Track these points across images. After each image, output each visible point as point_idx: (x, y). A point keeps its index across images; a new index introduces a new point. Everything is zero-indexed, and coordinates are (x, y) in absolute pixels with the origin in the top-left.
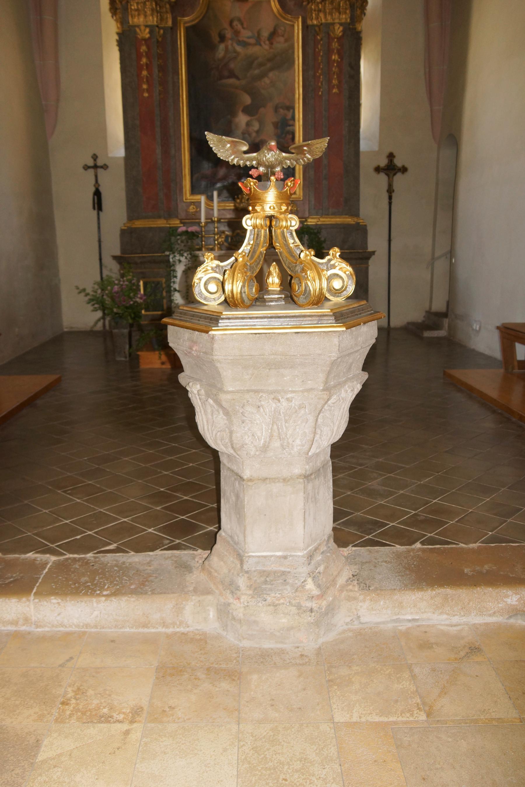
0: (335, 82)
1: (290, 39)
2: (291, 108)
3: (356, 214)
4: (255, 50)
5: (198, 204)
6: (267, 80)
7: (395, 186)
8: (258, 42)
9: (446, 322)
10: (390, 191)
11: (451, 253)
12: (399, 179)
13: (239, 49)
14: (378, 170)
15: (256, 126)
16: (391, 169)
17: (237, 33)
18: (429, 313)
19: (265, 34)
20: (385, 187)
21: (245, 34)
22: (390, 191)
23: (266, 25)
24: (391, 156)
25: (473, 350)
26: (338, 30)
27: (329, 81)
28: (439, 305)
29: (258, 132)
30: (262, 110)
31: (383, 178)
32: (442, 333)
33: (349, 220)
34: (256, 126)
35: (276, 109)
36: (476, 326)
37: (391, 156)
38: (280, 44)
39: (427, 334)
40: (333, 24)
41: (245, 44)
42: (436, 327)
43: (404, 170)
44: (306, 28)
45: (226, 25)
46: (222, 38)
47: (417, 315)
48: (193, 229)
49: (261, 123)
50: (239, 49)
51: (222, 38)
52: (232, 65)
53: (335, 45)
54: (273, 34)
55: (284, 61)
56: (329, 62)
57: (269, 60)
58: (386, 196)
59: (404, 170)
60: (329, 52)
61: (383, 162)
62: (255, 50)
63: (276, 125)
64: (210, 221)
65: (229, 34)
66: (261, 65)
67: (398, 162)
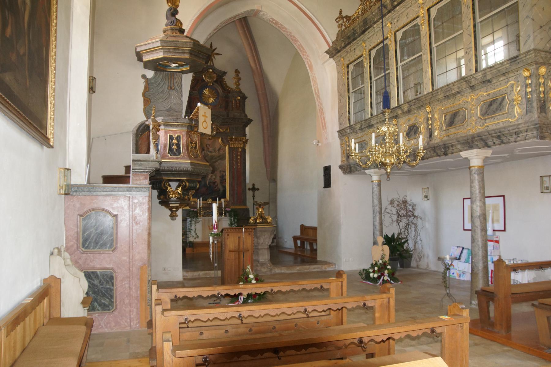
1: (225, 150)
2: (225, 172)
3: (245, 205)
4: (214, 154)
5: (196, 202)
6: (217, 163)
7: (255, 195)
8: (215, 151)
12: (256, 192)
13: (209, 153)
14: (249, 189)
15: (214, 177)
16: (254, 189)
17: (208, 148)
19: (217, 149)
21: (211, 149)
24: (254, 185)
26: (240, 150)
27: (237, 164)
30: (216, 172)
31: (251, 192)
33: (244, 207)
34: (214, 177)
35: (220, 172)
36: (286, 240)
37: (254, 185)
38: (221, 152)
40: (238, 148)
43: (258, 189)
44: (229, 148)
48: (195, 210)
49: (216, 176)
50: (209, 153)
53: (239, 154)
54: (219, 150)
55: (223, 157)
57: (219, 157)
58: (252, 198)
59: (258, 189)
60: (237, 156)
61: (251, 187)
62: (214, 154)
63: (220, 177)
64: (200, 207)
65: (206, 149)
66: (215, 158)
67: (256, 187)
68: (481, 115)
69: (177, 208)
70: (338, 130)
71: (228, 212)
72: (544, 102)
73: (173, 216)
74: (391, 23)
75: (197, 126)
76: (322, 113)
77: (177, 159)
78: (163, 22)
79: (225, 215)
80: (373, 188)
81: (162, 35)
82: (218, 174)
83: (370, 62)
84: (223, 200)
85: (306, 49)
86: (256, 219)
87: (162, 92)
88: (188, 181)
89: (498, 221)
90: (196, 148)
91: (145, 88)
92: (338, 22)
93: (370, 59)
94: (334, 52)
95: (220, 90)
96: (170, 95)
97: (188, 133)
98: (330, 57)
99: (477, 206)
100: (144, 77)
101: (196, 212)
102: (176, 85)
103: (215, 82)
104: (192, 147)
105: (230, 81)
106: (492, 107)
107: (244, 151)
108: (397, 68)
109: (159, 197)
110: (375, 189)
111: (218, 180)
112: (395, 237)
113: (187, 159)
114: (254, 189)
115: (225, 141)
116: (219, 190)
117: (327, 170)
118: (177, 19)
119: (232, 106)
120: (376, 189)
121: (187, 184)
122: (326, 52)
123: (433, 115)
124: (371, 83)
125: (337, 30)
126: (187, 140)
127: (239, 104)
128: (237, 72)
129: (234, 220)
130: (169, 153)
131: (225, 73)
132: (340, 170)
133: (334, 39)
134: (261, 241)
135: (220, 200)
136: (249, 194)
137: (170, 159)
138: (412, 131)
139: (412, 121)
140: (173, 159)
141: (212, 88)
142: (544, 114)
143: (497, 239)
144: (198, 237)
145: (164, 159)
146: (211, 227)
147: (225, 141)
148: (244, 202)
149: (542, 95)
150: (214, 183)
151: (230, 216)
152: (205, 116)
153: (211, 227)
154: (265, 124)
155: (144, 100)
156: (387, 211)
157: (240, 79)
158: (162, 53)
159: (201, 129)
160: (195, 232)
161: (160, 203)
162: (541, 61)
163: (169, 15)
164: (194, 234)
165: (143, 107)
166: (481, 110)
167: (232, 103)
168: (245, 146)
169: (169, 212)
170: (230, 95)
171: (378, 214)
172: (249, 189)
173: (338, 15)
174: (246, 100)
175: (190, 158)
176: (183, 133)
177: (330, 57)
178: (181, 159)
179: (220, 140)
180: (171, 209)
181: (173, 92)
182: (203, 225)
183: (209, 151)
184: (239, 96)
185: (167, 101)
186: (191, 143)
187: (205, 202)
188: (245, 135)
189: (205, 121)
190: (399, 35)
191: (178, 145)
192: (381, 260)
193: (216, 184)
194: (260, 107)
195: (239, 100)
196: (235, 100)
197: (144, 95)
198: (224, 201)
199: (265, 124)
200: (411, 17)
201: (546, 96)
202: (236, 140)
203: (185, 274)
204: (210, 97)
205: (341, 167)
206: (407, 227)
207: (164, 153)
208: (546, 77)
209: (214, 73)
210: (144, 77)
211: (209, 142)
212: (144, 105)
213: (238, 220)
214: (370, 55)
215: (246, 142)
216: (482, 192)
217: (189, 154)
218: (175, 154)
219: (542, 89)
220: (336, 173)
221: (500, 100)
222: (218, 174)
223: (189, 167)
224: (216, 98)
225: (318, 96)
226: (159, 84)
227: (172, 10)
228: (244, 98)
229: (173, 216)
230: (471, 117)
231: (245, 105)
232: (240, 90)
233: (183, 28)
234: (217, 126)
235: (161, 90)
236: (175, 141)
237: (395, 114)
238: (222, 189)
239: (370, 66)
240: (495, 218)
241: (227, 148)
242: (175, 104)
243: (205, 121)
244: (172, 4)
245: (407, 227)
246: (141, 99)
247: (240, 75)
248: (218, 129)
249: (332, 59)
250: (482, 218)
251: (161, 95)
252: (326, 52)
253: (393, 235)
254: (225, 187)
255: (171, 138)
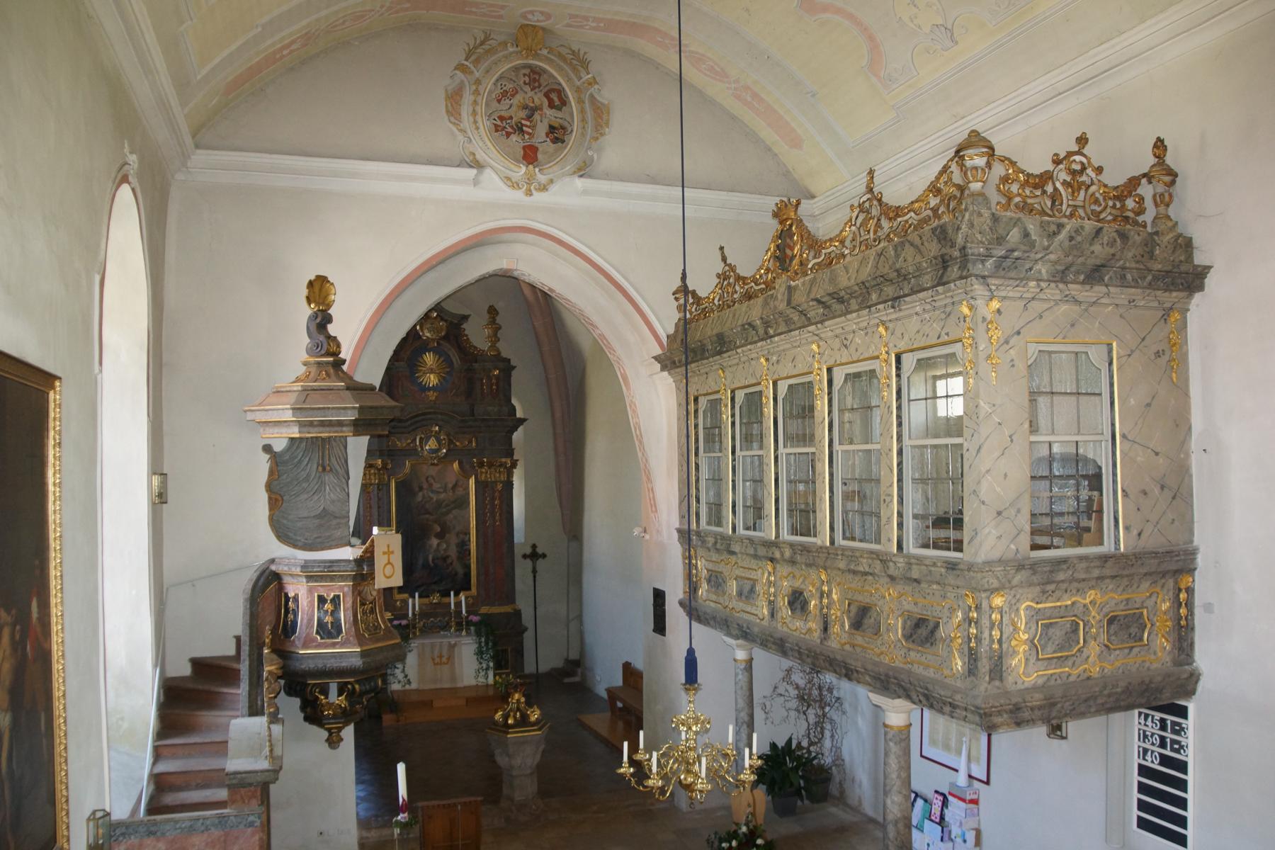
0: (497, 517)
2: (468, 533)
5: (405, 602)
6: (451, 516)
7: (538, 569)
8: (445, 491)
9: (579, 671)
10: (534, 571)
11: (580, 617)
12: (540, 562)
14: (525, 556)
16: (534, 555)
17: (431, 485)
18: (567, 661)
19: (450, 486)
20: (530, 569)
21: (436, 486)
22: (534, 571)
23: (451, 480)
24: (534, 546)
25: (597, 695)
26: (500, 487)
28: (574, 655)
29: (445, 550)
31: (529, 562)
32: (577, 679)
35: (457, 535)
36: (598, 678)
37: (534, 546)
38: (460, 492)
39: (567, 680)
40: (495, 482)
41: (438, 492)
42: (573, 674)
43: (544, 556)
45: (423, 479)
46: (421, 489)
47: (559, 663)
48: (404, 622)
51: (421, 489)
52: (427, 506)
54: (454, 488)
55: (464, 502)
56: (493, 506)
59: (544, 556)
60: (493, 499)
61: (528, 551)
62: (442, 496)
65: (425, 486)
67: (539, 551)
68: (903, 635)
69: (340, 729)
70: (677, 526)
71: (475, 624)
72: (1000, 657)
73: (333, 742)
74: (767, 360)
75: (371, 575)
76: (649, 480)
77: (334, 645)
78: (302, 340)
79: (468, 634)
80: (736, 675)
81: (305, 357)
82: (453, 539)
83: (733, 416)
84: (462, 597)
85: (615, 344)
86: (506, 717)
87: (307, 479)
88: (357, 682)
89: (978, 761)
90: (372, 611)
91: (271, 473)
92: (676, 299)
93: (733, 407)
94: (666, 362)
95: (456, 359)
96: (323, 484)
97: (357, 592)
98: (663, 369)
99: (893, 802)
100: (267, 449)
101: (407, 626)
102: (333, 460)
103: (444, 338)
104: (364, 613)
105: (477, 334)
106: (919, 631)
107: (509, 485)
108: (776, 458)
109: (303, 708)
110: (740, 677)
111: (453, 552)
112: (794, 746)
113: (354, 646)
114: (534, 555)
115: (467, 467)
116: (456, 574)
117: (659, 596)
118: (329, 337)
119: (482, 389)
120: (742, 677)
121: (357, 686)
122: (656, 358)
123: (830, 591)
124: (734, 460)
125: (676, 316)
126: (354, 603)
127: (497, 384)
128: (493, 311)
129: (487, 644)
130: (318, 633)
131: (465, 318)
132: (681, 610)
133: (671, 331)
134: (517, 761)
135: (457, 594)
136: (522, 570)
137: (319, 646)
138: (797, 601)
139: (797, 584)
140: (326, 646)
141: (437, 351)
142: (997, 683)
143: (975, 797)
144: (409, 682)
145: (308, 648)
146: (437, 660)
147: (467, 467)
148: (510, 598)
149: (996, 646)
150: (445, 559)
151: (478, 634)
152: (389, 553)
153: (437, 660)
154: (558, 415)
155: (270, 498)
156: (779, 691)
157: (500, 328)
158: (296, 429)
159: (381, 582)
160: (403, 671)
161: (306, 719)
162: (996, 584)
163: (313, 328)
164: (400, 676)
165: (267, 512)
166: (904, 628)
167: (482, 385)
168: (510, 474)
169: (325, 734)
170: (476, 366)
171: (745, 726)
172: (525, 556)
173: (678, 283)
174: (514, 373)
175: (360, 645)
176: (346, 589)
177: (663, 369)
178: (342, 645)
179: (456, 465)
180: (329, 730)
181: (329, 478)
182: (421, 656)
183: (433, 491)
184: (496, 368)
185: (316, 497)
186: (363, 604)
187: (426, 600)
188: (510, 453)
189: (389, 563)
190: (783, 387)
191: (335, 612)
192: (747, 825)
193: (449, 561)
194: (547, 379)
195: (497, 377)
196: (489, 378)
197: (269, 487)
198: (466, 598)
199: (558, 415)
200: (801, 368)
201: (1005, 646)
202: (490, 465)
203: (365, 834)
204: (432, 371)
205: (681, 603)
206: (819, 724)
207: (308, 634)
208: (1006, 609)
209: (442, 319)
210: (267, 449)
211: (433, 471)
212: (270, 510)
213: (495, 644)
214: (733, 399)
215: (514, 465)
216: (903, 775)
217: (357, 630)
218: (330, 635)
219: (996, 634)
220: (675, 615)
221: (931, 625)
222: (453, 539)
223: (357, 662)
224: (448, 373)
225: (641, 442)
226: (300, 461)
227: (318, 320)
228: (507, 368)
229: (333, 742)
230: (888, 630)
231: (510, 385)
232: (499, 353)
233: (342, 356)
234: (448, 435)
235: (304, 474)
236: (328, 606)
237: (770, 555)
238: (461, 571)
239: (733, 424)
240: (973, 753)
241: (472, 481)
242: (333, 502)
243: (389, 563)
244: (317, 304)
245: (819, 724)
246: (264, 496)
247: (498, 320)
248: (450, 442)
249: (665, 374)
250: (901, 826)
251: (305, 485)
252: (656, 358)
253: (790, 741)
254: (468, 567)
255: (322, 600)
